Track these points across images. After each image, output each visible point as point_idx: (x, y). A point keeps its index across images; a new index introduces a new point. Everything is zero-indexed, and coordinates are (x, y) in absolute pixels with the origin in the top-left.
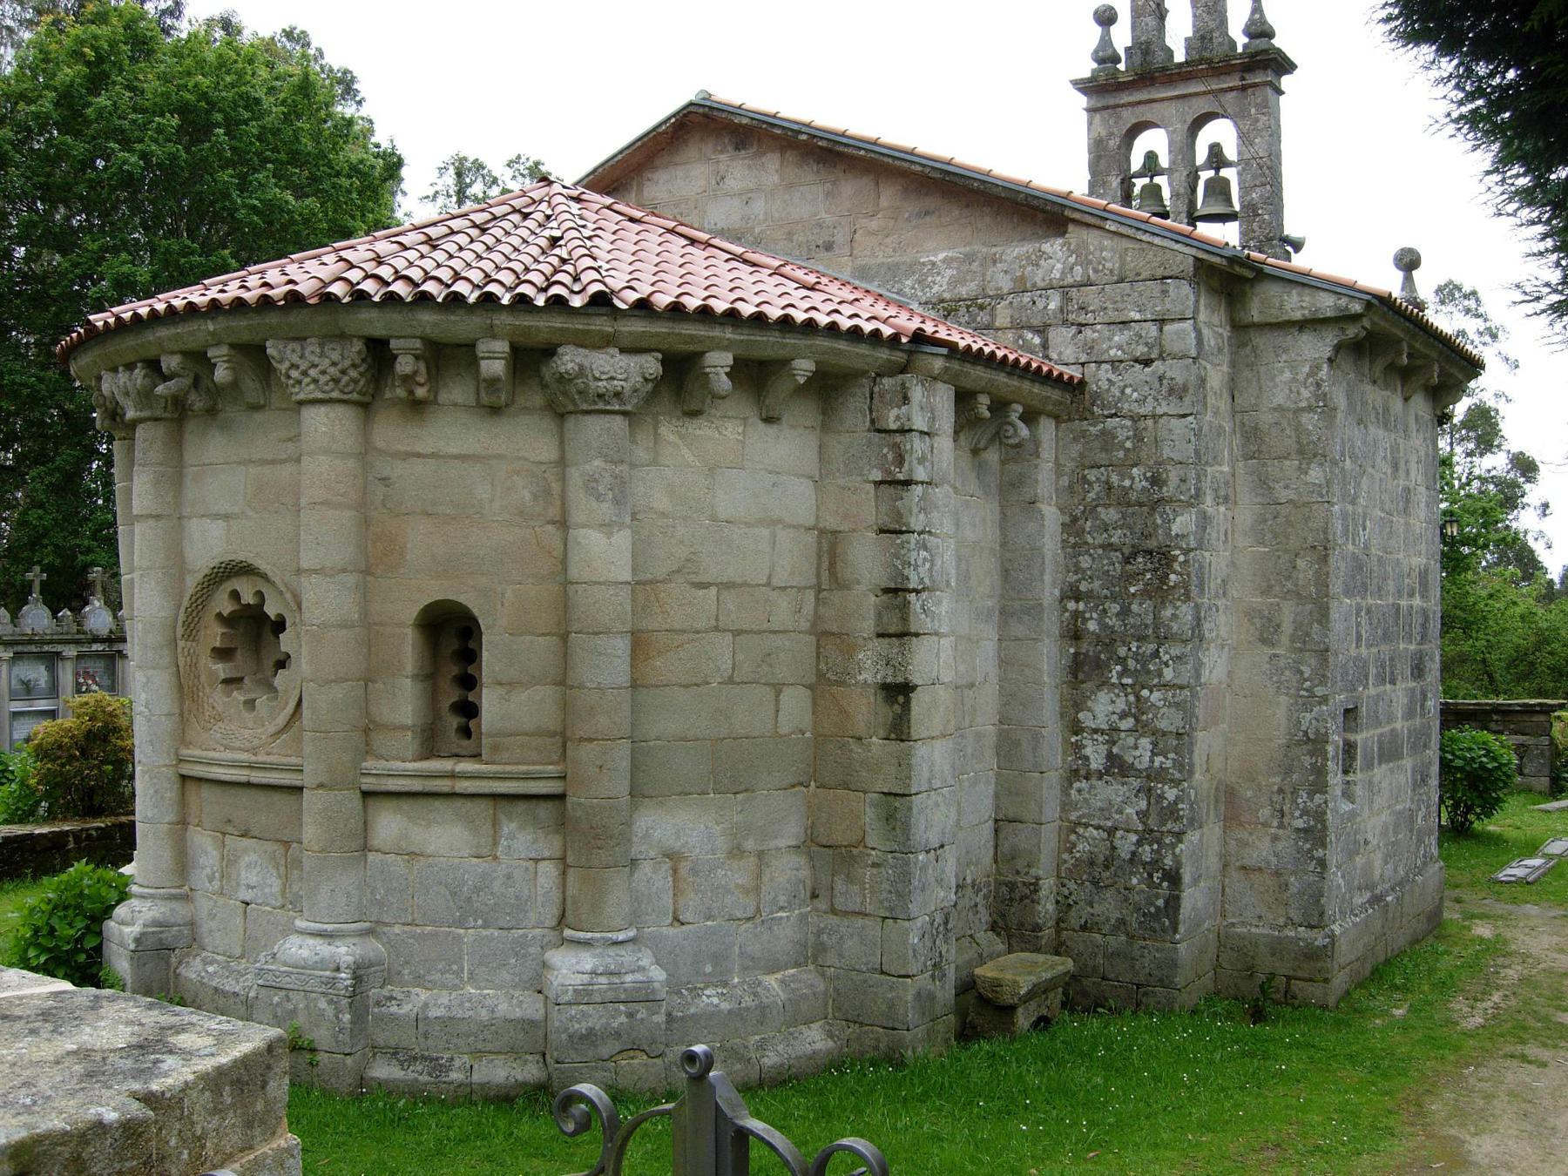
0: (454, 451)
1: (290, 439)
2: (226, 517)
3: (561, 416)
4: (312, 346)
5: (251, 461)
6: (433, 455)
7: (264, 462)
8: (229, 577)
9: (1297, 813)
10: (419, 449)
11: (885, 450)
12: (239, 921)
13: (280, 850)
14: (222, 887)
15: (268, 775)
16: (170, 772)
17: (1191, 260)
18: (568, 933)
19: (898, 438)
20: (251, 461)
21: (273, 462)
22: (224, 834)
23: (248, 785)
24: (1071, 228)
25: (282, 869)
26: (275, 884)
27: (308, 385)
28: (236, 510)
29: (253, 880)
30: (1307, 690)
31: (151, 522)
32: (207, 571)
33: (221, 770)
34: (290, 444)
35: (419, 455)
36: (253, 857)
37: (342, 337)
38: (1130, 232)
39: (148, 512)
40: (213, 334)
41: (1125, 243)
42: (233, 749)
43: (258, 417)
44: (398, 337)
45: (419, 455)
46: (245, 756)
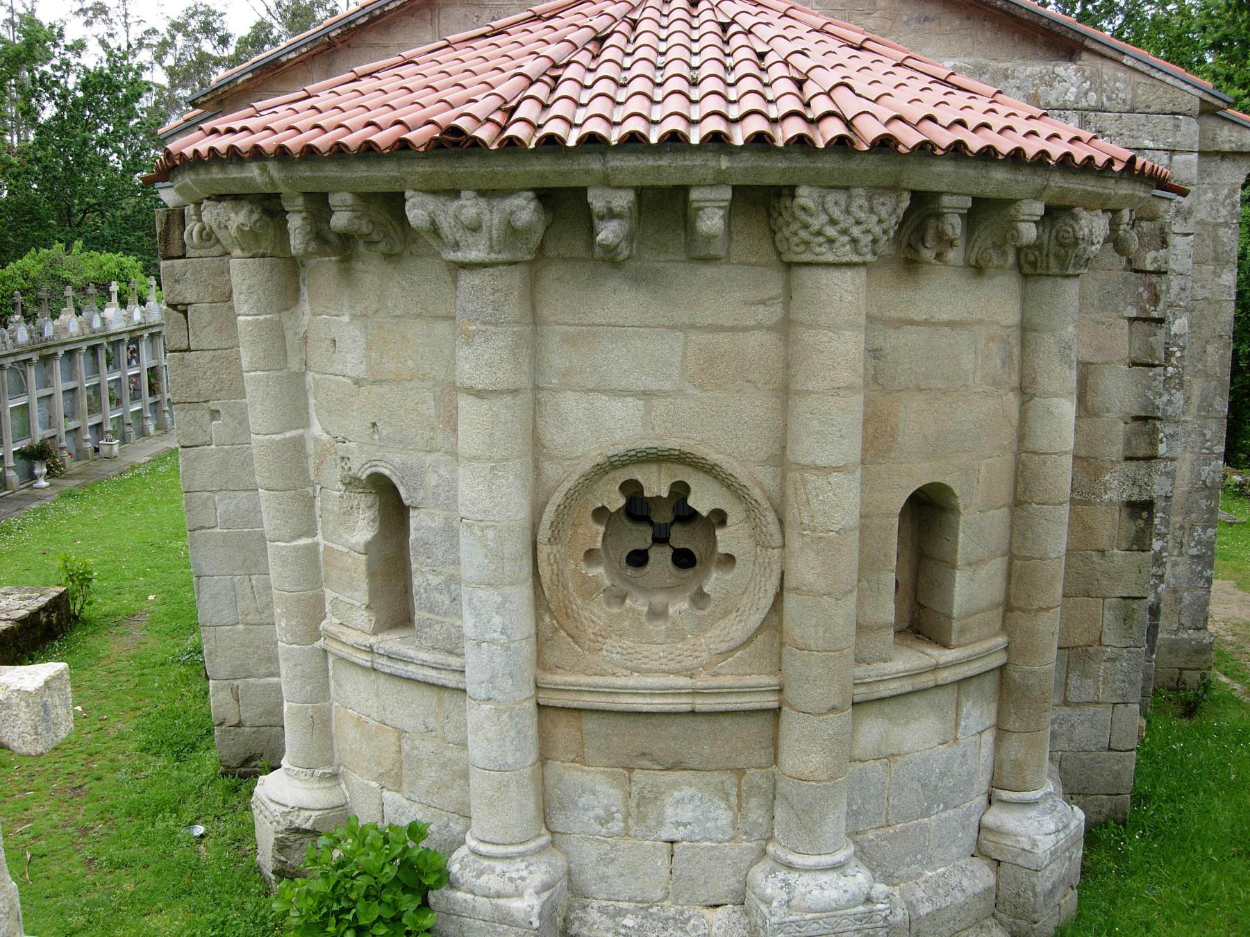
0: (945, 317)
1: (763, 302)
2: (646, 394)
3: (1025, 276)
4: (860, 200)
5: (693, 327)
6: (927, 323)
7: (715, 329)
8: (624, 465)
9: (1193, 544)
10: (913, 314)
11: (1141, 290)
12: (662, 862)
13: (729, 780)
14: (627, 828)
15: (720, 700)
16: (530, 706)
17: (1198, 101)
18: (1005, 795)
19: (1154, 279)
20: (693, 327)
21: (732, 329)
22: (631, 770)
23: (693, 713)
24: (1085, 56)
25: (734, 800)
26: (723, 816)
27: (844, 245)
28: (667, 385)
29: (687, 814)
30: (1207, 449)
31: (508, 399)
32: (600, 460)
33: (640, 700)
34: (761, 308)
35: (912, 323)
36: (687, 791)
37: (895, 189)
38: (1145, 69)
39: (505, 386)
40: (720, 172)
41: (1142, 79)
42: (649, 672)
43: (708, 271)
44: (952, 194)
45: (912, 323)
46: (682, 681)
